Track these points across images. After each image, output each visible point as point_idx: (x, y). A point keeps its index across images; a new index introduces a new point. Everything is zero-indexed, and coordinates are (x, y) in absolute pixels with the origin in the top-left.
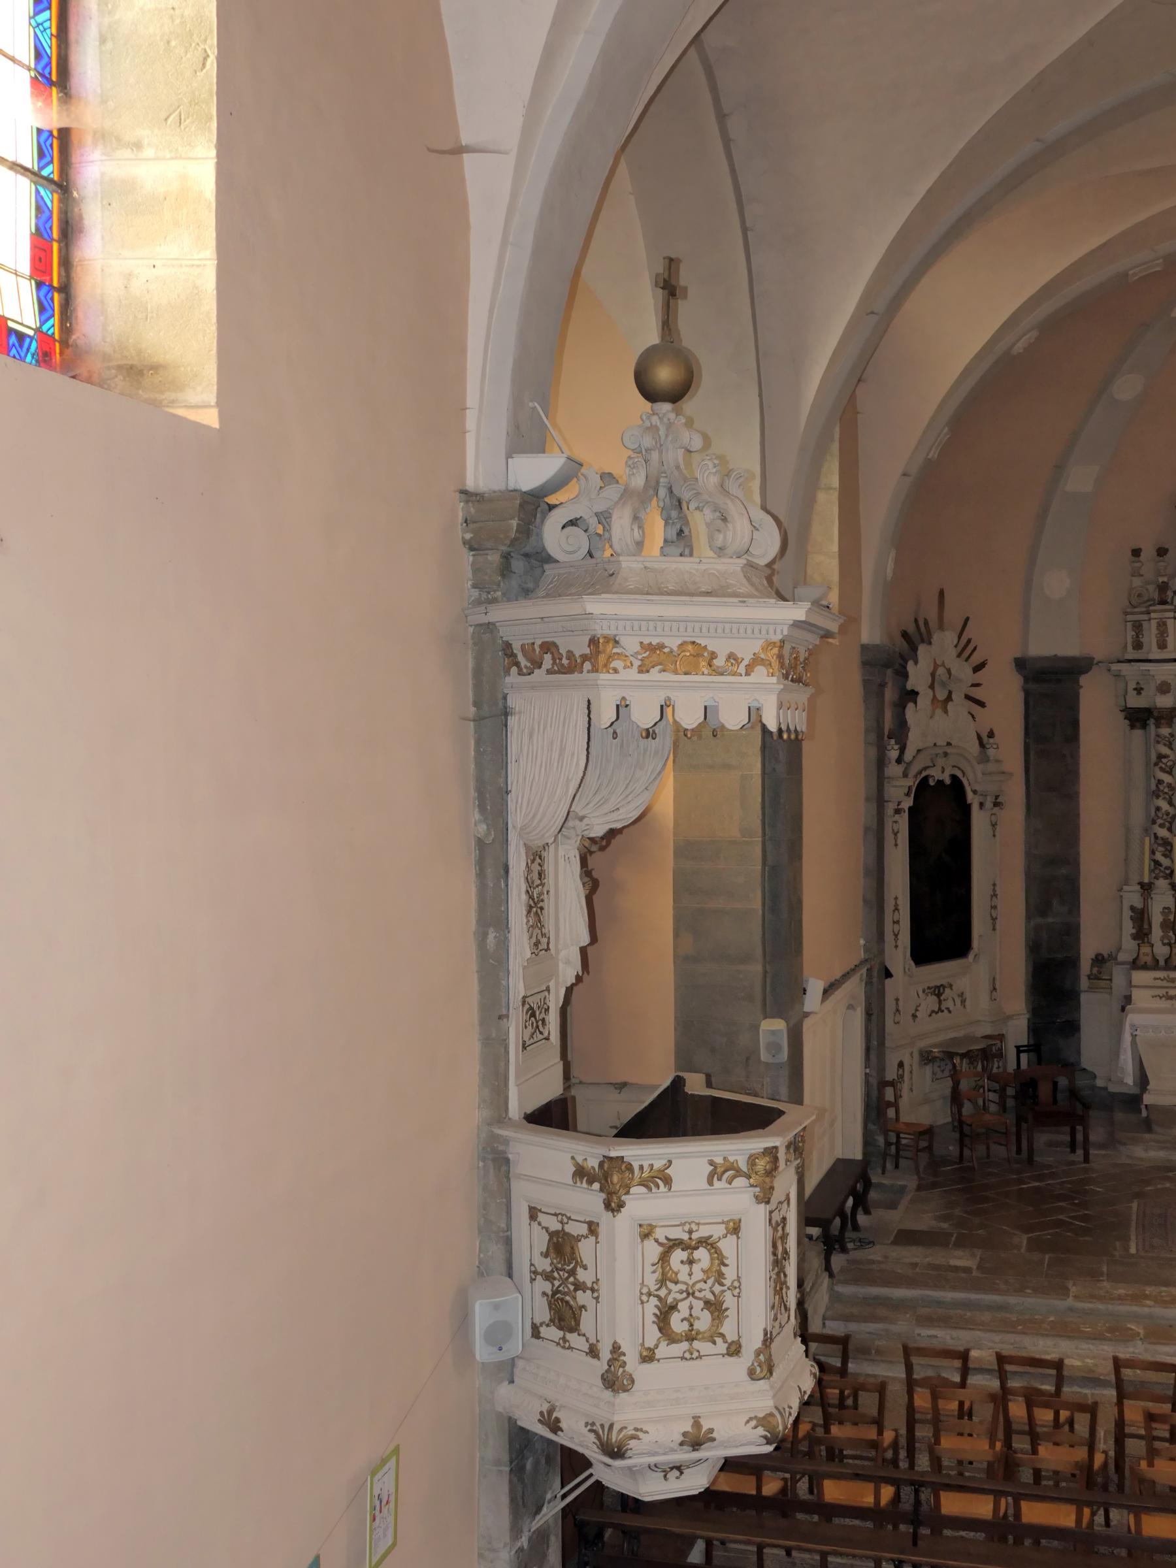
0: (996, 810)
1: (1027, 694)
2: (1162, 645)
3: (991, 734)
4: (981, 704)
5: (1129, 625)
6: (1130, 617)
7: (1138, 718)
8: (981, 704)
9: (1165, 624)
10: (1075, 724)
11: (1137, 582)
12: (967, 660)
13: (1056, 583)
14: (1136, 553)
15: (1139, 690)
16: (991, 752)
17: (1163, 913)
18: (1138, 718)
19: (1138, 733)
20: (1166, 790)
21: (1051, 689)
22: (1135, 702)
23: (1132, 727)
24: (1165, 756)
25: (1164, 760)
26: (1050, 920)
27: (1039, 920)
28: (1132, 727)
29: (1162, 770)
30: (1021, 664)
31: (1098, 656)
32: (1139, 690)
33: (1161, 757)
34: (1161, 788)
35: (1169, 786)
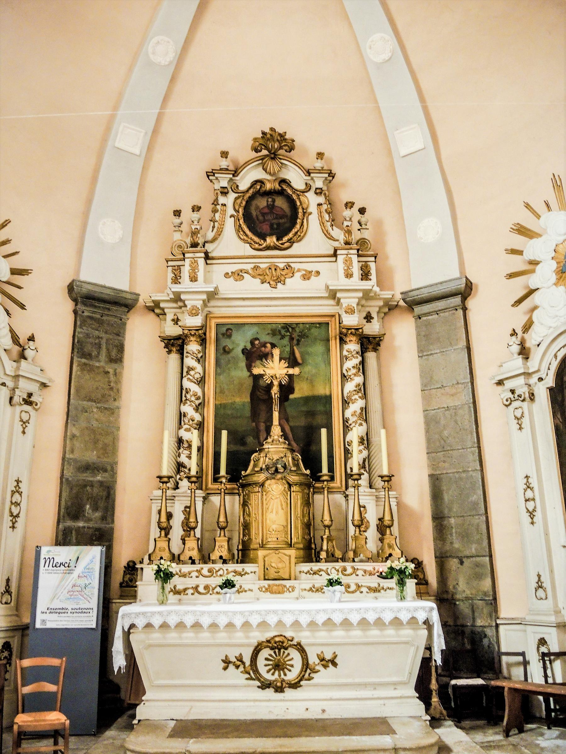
0: (27, 408)
1: (75, 312)
2: (193, 279)
3: (31, 339)
4: (22, 307)
5: (170, 268)
6: (170, 263)
7: (175, 344)
8: (22, 307)
9: (196, 262)
10: (121, 348)
11: (177, 236)
12: (5, 257)
13: (109, 229)
14: (177, 213)
15: (176, 321)
16: (29, 353)
17: (184, 512)
18: (175, 344)
19: (174, 357)
20: (193, 399)
21: (100, 314)
22: (173, 331)
23: (169, 352)
24: (192, 369)
25: (192, 373)
26: (81, 524)
27: (69, 523)
28: (169, 352)
29: (189, 379)
30: (71, 288)
31: (144, 299)
32: (176, 321)
33: (190, 369)
34: (188, 396)
35: (195, 395)
